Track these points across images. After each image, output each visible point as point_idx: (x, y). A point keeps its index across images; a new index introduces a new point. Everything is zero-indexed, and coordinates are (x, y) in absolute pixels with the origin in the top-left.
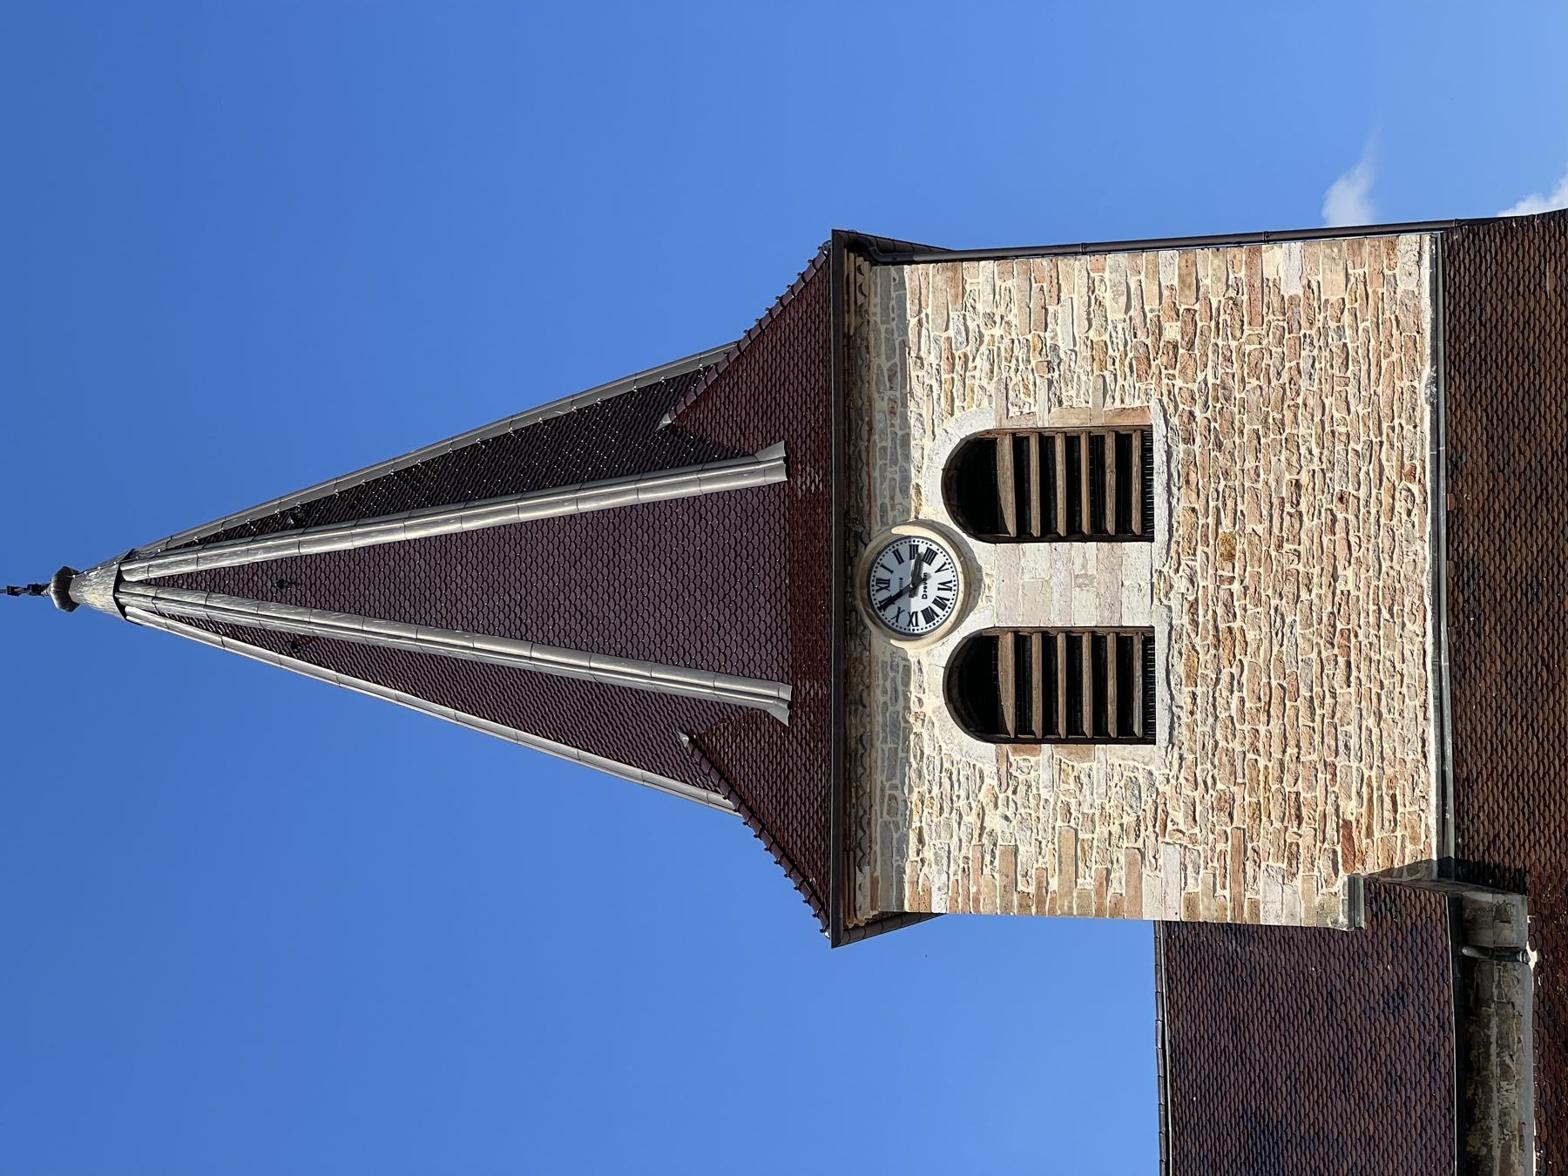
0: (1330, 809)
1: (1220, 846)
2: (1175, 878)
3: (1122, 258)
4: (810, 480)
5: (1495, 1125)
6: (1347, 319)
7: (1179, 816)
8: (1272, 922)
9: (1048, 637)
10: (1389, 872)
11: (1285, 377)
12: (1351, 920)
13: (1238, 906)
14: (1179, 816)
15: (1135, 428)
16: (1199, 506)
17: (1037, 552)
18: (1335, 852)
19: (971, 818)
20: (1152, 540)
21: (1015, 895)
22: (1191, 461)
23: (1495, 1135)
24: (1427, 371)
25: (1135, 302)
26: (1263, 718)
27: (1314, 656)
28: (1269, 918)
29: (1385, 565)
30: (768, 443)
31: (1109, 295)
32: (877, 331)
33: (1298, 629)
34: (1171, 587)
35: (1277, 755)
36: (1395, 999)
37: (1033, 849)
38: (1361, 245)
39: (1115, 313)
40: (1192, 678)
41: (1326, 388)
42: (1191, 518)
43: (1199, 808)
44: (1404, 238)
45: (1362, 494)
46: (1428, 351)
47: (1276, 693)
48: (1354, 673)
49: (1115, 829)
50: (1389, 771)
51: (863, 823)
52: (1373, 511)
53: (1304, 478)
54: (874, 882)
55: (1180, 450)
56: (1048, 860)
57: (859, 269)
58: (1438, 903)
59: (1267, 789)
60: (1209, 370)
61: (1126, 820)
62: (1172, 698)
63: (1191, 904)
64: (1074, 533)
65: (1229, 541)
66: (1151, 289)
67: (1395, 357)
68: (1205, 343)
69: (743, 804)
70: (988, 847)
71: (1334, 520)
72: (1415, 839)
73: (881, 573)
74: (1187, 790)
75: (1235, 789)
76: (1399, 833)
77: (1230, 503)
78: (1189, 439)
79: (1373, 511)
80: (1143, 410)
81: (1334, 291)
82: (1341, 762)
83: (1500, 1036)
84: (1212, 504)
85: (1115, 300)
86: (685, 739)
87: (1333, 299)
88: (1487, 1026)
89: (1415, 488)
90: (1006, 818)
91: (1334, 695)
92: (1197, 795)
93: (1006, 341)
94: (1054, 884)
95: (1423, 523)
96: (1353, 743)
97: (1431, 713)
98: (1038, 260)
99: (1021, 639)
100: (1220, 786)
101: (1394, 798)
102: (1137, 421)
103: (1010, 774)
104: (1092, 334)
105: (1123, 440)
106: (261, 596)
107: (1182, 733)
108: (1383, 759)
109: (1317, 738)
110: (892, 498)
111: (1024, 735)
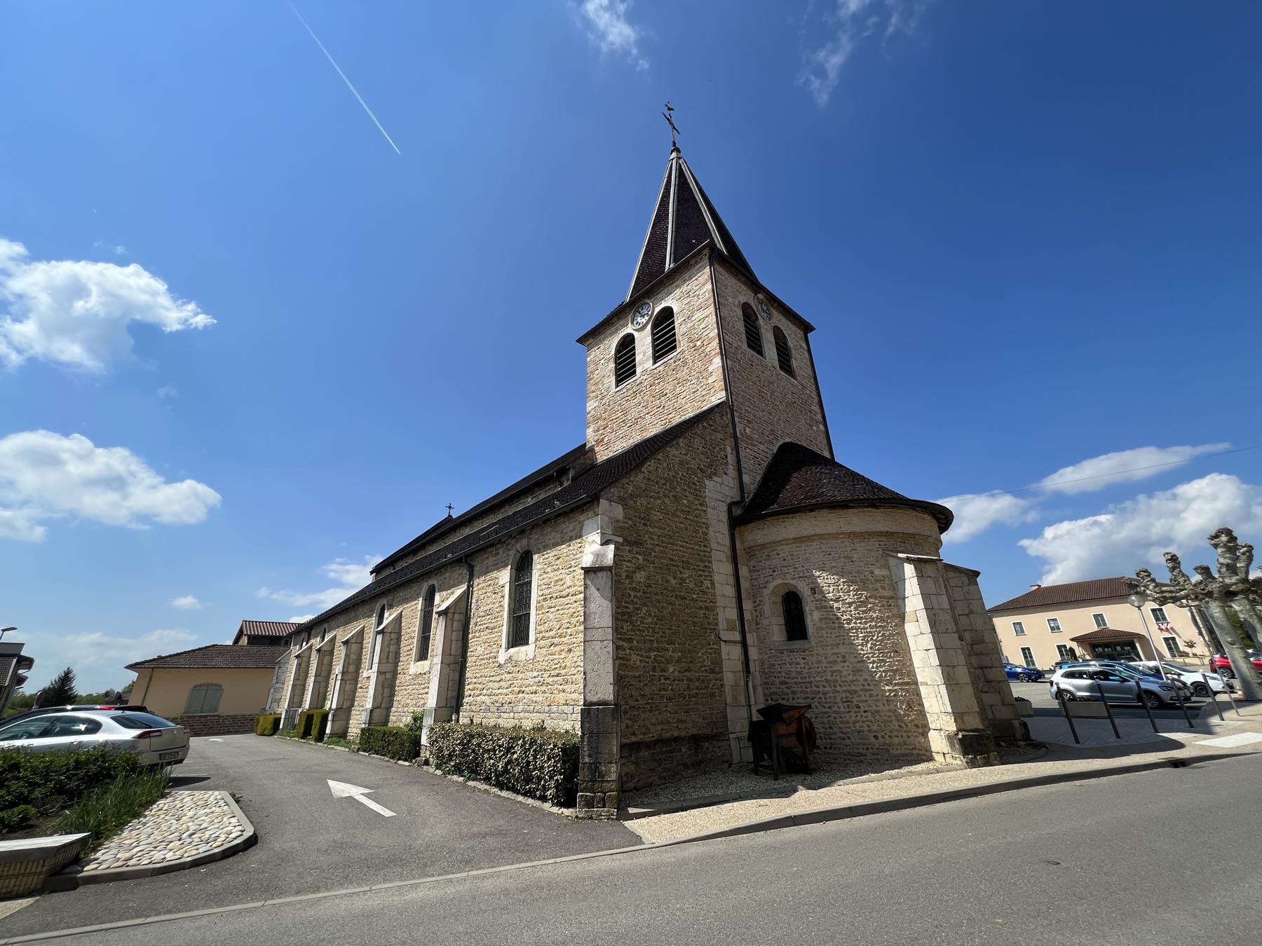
55: (672, 361)
57: (706, 255)
106: (666, 184)
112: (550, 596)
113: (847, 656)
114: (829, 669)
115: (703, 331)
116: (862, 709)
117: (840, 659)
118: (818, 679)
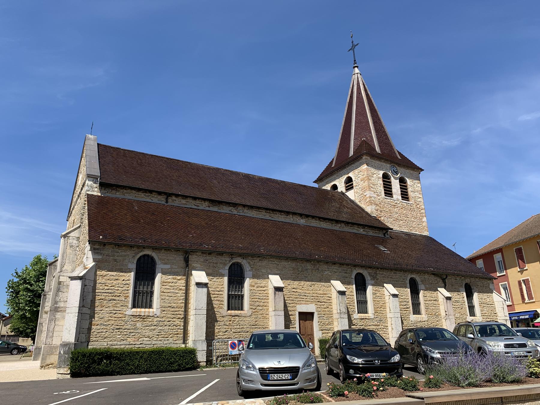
5: (368, 230)
14: (379, 198)
16: (405, 206)
18: (378, 215)
23: (367, 230)
24: (419, 234)
25: (420, 202)
35: (386, 210)
54: (368, 159)
71: (406, 221)
73: (394, 167)
74: (381, 199)
78: (410, 206)
89: (410, 231)
91: (392, 218)
94: (370, 181)
96: (388, 220)
103: (380, 178)
104: (417, 197)
107: (386, 200)
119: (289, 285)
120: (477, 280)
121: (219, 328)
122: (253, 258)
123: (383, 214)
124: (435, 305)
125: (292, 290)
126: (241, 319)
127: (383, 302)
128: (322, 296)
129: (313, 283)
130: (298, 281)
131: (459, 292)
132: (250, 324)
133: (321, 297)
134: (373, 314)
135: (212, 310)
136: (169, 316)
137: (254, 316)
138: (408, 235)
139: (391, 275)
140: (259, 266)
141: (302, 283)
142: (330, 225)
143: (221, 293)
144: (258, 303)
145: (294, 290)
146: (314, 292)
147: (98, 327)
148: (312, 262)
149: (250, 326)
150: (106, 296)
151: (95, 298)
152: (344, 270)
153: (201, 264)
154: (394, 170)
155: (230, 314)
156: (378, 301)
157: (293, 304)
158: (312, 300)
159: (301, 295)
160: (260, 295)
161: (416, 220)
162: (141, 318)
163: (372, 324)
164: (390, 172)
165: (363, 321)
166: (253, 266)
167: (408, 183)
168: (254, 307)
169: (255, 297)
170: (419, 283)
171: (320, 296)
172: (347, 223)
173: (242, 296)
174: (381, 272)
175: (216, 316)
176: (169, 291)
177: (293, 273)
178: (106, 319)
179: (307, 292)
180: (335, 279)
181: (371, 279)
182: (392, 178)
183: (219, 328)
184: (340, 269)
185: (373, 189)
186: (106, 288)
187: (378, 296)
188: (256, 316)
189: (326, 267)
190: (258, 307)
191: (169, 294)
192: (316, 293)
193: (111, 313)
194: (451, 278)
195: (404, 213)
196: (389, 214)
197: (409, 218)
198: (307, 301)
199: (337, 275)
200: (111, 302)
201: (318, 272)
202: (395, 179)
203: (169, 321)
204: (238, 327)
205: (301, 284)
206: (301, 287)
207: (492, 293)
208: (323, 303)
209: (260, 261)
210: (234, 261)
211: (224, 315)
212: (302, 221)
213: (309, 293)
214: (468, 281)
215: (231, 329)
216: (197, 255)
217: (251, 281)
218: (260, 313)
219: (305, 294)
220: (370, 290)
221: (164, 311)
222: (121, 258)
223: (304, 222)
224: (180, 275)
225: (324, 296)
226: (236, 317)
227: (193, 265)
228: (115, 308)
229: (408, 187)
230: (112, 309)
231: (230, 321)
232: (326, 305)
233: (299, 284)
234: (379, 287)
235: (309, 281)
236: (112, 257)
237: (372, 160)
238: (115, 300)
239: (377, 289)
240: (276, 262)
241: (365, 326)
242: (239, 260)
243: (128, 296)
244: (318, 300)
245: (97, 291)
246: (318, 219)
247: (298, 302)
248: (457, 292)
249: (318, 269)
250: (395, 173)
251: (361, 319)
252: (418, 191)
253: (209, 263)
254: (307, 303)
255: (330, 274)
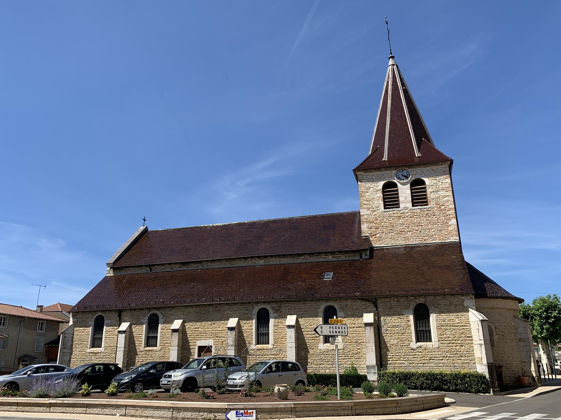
0: (377, 233)
1: (371, 219)
2: (366, 213)
3: (452, 200)
4: (417, 160)
6: (446, 231)
7: (375, 213)
8: (362, 226)
9: (398, 194)
10: (370, 240)
11: (437, 223)
12: (363, 236)
13: (363, 222)
14: (375, 213)
15: (428, 203)
16: (418, 213)
17: (409, 191)
19: (372, 186)
20: (412, 207)
21: (361, 193)
22: (424, 211)
23: (338, 256)
24: (439, 242)
26: (389, 223)
27: (398, 229)
28: (362, 226)
29: (412, 238)
30: (421, 153)
31: (447, 198)
32: (439, 167)
33: (402, 227)
34: (406, 210)
35: (384, 225)
36: (353, 242)
37: (368, 195)
38: (457, 232)
39: (444, 199)
40: (394, 214)
41: (436, 229)
42: (416, 212)
43: (376, 216)
44: (458, 237)
45: (421, 234)
46: (442, 242)
47: (393, 225)
48: (396, 235)
49: (372, 205)
50: (383, 240)
51: (370, 172)
52: (419, 236)
53: (423, 227)
54: (362, 174)
56: (367, 197)
57: (448, 163)
58: (367, 247)
59: (379, 224)
60: (437, 213)
61: (373, 206)
62: (391, 211)
63: (363, 216)
64: (412, 196)
65: (413, 217)
66: (448, 204)
67: (441, 237)
68: (441, 212)
69: (370, 155)
70: (368, 189)
71: (417, 231)
72: (374, 244)
73: (404, 171)
74: (378, 214)
75: (379, 220)
76: (375, 242)
77: (418, 217)
79: (419, 236)
80: (431, 204)
81: (450, 229)
82: (384, 234)
83: (350, 256)
84: (418, 215)
85: (446, 199)
86: (379, 147)
87: (449, 229)
88: (352, 254)
89: (423, 241)
90: (372, 191)
91: (393, 232)
92: (378, 215)
93: (439, 185)
94: (363, 198)
95: (418, 242)
96: (387, 235)
97: (392, 245)
98: (451, 188)
99: (397, 190)
100: (379, 218)
101: (380, 241)
102: (429, 204)
103: (378, 191)
105: (426, 202)
106: (393, 85)
107: (386, 213)
108: (385, 239)
109: (387, 230)
110: (415, 171)
111: (383, 192)
112: (446, 325)
113: (506, 351)
114: (500, 356)
115: (445, 202)
116: (510, 370)
117: (504, 353)
118: (497, 359)
119: (192, 326)
120: (438, 298)
121: (138, 359)
122: (164, 309)
123: (380, 230)
124: (358, 332)
125: (195, 330)
126: (153, 353)
127: (285, 333)
128: (221, 332)
129: (214, 322)
130: (200, 322)
131: (402, 315)
132: (159, 356)
133: (219, 333)
134: (272, 344)
135: (134, 347)
136: (109, 352)
137: (163, 351)
138: (410, 249)
139: (299, 306)
140: (170, 314)
141: (204, 323)
142: (291, 259)
143: (141, 336)
144: (166, 341)
145: (196, 329)
146: (213, 329)
147: (74, 359)
148: (214, 305)
149: (159, 358)
150: (78, 342)
151: (73, 343)
152: (245, 308)
153: (129, 318)
154: (402, 175)
155: (146, 350)
156: (280, 332)
157: (194, 341)
158: (211, 336)
159: (201, 333)
160: (168, 335)
161: (437, 225)
162: (94, 354)
163: (270, 353)
164: (395, 180)
165: (260, 351)
166: (164, 315)
167: (427, 184)
168: (163, 345)
169: (164, 337)
170: (338, 310)
171: (219, 332)
172: (311, 254)
173: (157, 337)
174: (286, 305)
175: (137, 352)
176: (110, 336)
177: (196, 316)
178: (78, 355)
179: (207, 330)
180: (235, 316)
181: (274, 313)
182: (399, 185)
183: (138, 359)
184: (241, 308)
185: (366, 206)
186: (78, 337)
187: (281, 328)
188: (164, 351)
189: (227, 307)
190: (166, 344)
191: (110, 339)
192: (216, 330)
193: (80, 351)
194: (390, 301)
195: (415, 221)
196: (389, 229)
197: (423, 227)
198: (207, 337)
199: (237, 313)
200: (80, 345)
201: (219, 312)
202: (404, 184)
203: (109, 355)
204: (151, 358)
205: (203, 324)
206: (202, 327)
207: (469, 312)
208: (221, 338)
209: (170, 311)
210: (151, 313)
211: (142, 350)
212: (260, 261)
213: (209, 331)
214: (421, 300)
215: (146, 360)
216: (127, 312)
217: (162, 326)
218: (167, 348)
219: (205, 332)
220: (272, 321)
221: (106, 349)
222: (85, 319)
223: (263, 262)
224: (116, 326)
225: (223, 332)
226: (150, 352)
227: (124, 318)
228: (82, 349)
229: (427, 188)
230: (80, 349)
231: (146, 354)
232: (224, 339)
233: (201, 325)
234: (283, 319)
235: (210, 321)
236: (81, 319)
237: (368, 174)
238: (82, 344)
239: (280, 321)
240: (182, 309)
241: (262, 356)
242: (155, 312)
243: (88, 341)
244: (216, 336)
245: (74, 339)
246: (277, 257)
247: (198, 339)
248: (398, 315)
249: (219, 310)
250: (404, 178)
251: (258, 349)
252: (443, 189)
253: (134, 316)
254: (206, 338)
255: (231, 313)
